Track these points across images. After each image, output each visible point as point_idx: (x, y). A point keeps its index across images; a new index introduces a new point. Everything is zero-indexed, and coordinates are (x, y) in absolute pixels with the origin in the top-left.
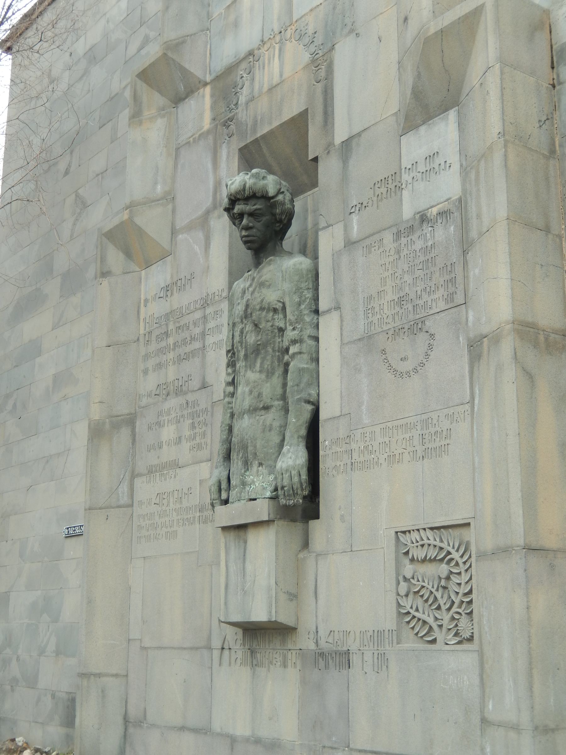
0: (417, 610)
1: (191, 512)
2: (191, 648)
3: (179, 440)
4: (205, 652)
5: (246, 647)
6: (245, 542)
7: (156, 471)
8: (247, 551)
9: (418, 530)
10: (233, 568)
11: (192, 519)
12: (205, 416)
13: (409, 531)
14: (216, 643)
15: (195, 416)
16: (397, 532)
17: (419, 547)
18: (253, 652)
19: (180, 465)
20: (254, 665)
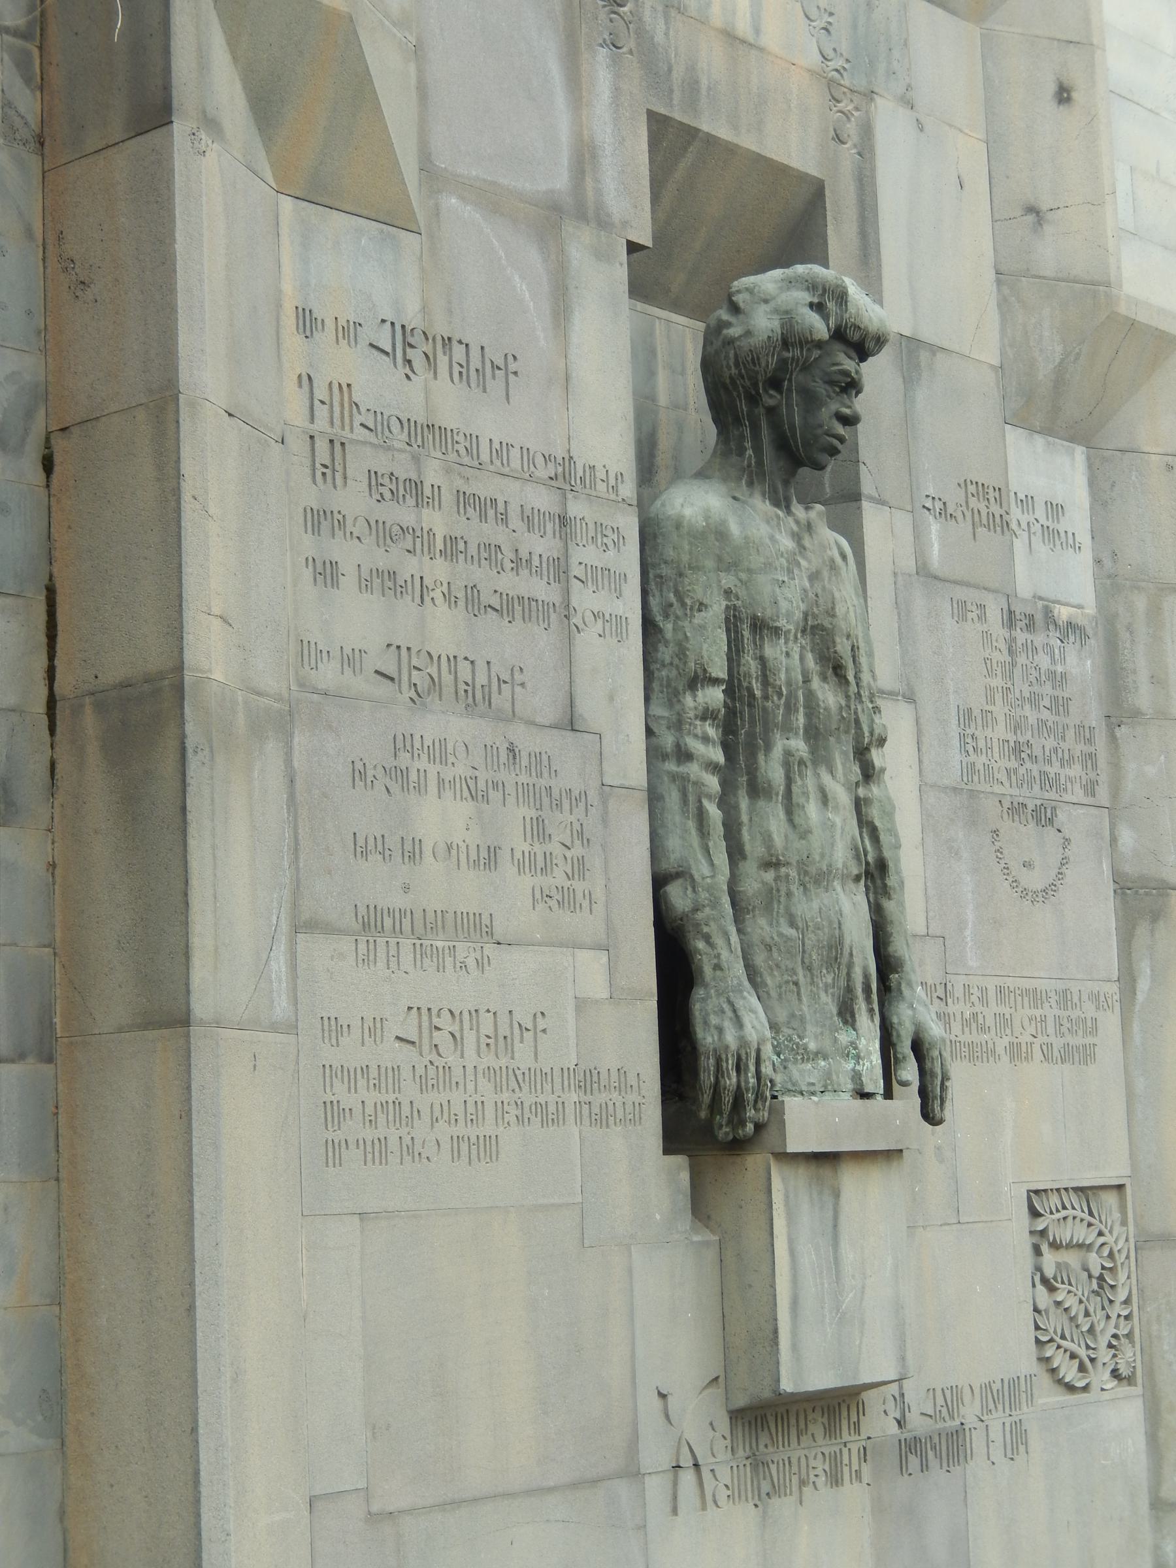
0: (1063, 1337)
1: (548, 1087)
2: (574, 1485)
3: (490, 858)
4: (622, 1488)
5: (741, 1453)
6: (837, 1194)
7: (398, 931)
8: (843, 1218)
9: (1058, 1190)
10: (808, 1258)
11: (552, 1108)
12: (580, 811)
13: (1045, 1191)
14: (655, 1454)
15: (546, 800)
16: (1028, 1191)
17: (1085, 1223)
18: (758, 1464)
19: (497, 937)
20: (764, 1495)
